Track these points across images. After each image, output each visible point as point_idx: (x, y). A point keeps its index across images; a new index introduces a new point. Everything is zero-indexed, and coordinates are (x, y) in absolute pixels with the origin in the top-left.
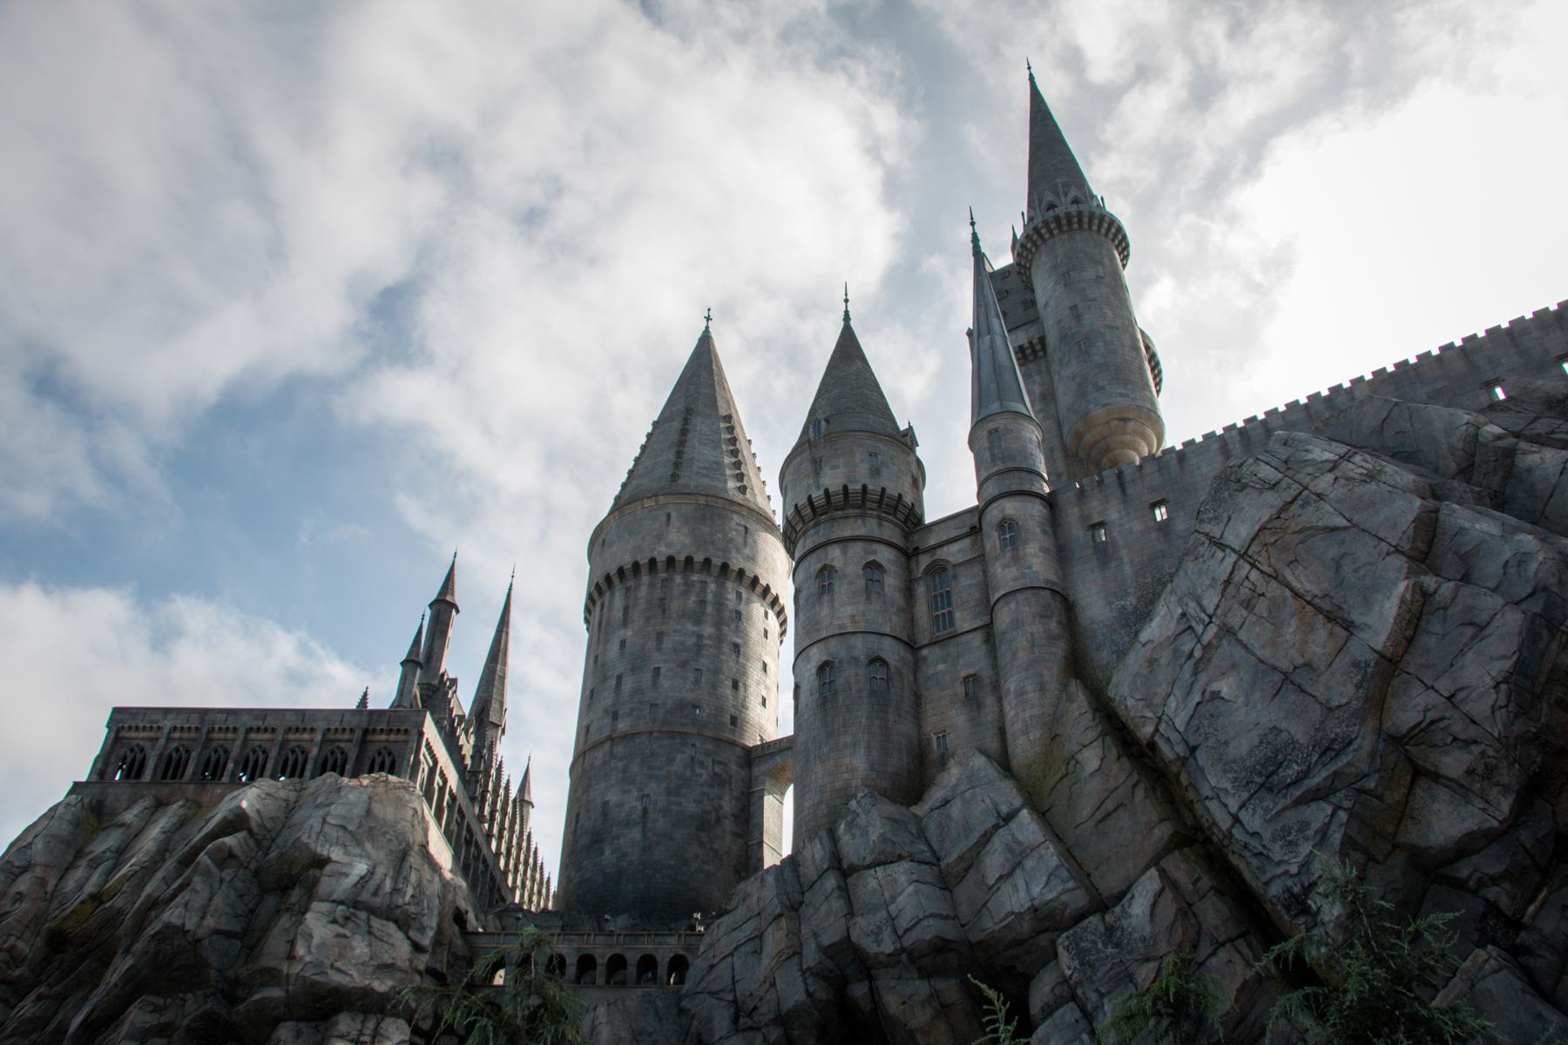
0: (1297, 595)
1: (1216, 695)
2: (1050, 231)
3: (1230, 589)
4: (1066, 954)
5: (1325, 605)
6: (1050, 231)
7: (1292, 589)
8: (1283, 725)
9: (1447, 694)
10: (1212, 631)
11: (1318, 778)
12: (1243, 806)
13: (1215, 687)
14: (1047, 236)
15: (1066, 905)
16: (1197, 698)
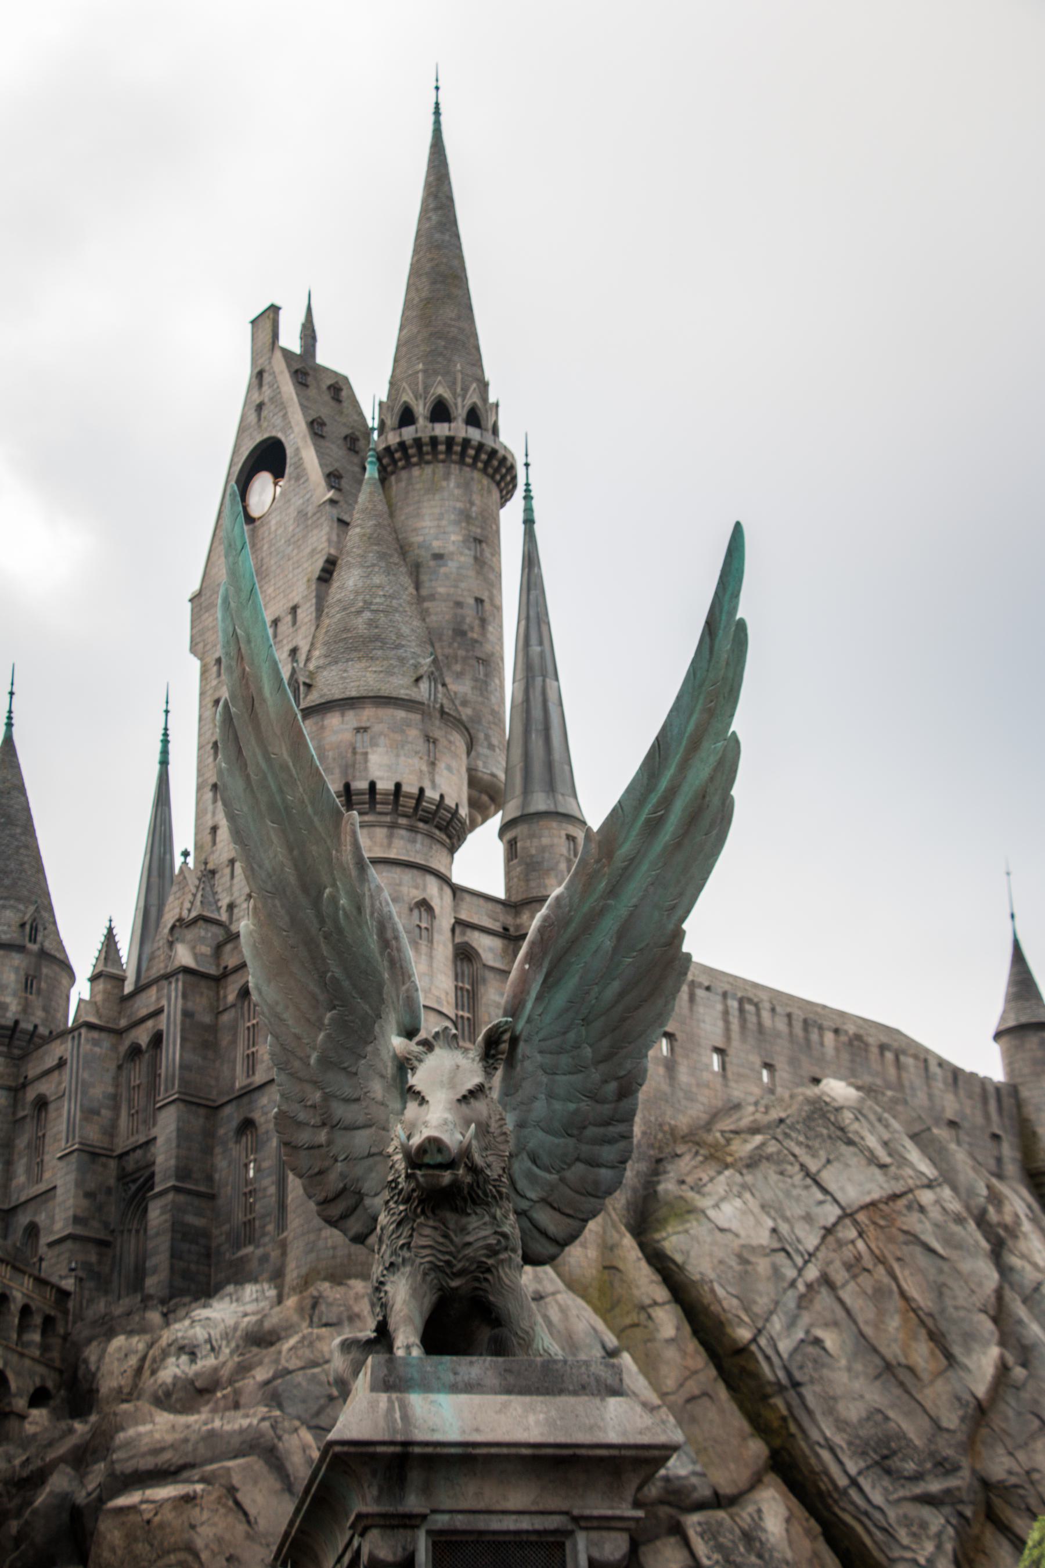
0: (903, 1294)
1: (818, 1342)
2: (476, 458)
3: (830, 1239)
4: (699, 1540)
5: (929, 1322)
6: (476, 458)
7: (899, 1286)
8: (891, 1414)
9: (1026, 1468)
10: (812, 1273)
11: (935, 1486)
12: (860, 1473)
13: (819, 1333)
14: (469, 460)
15: (694, 1488)
16: (801, 1335)
